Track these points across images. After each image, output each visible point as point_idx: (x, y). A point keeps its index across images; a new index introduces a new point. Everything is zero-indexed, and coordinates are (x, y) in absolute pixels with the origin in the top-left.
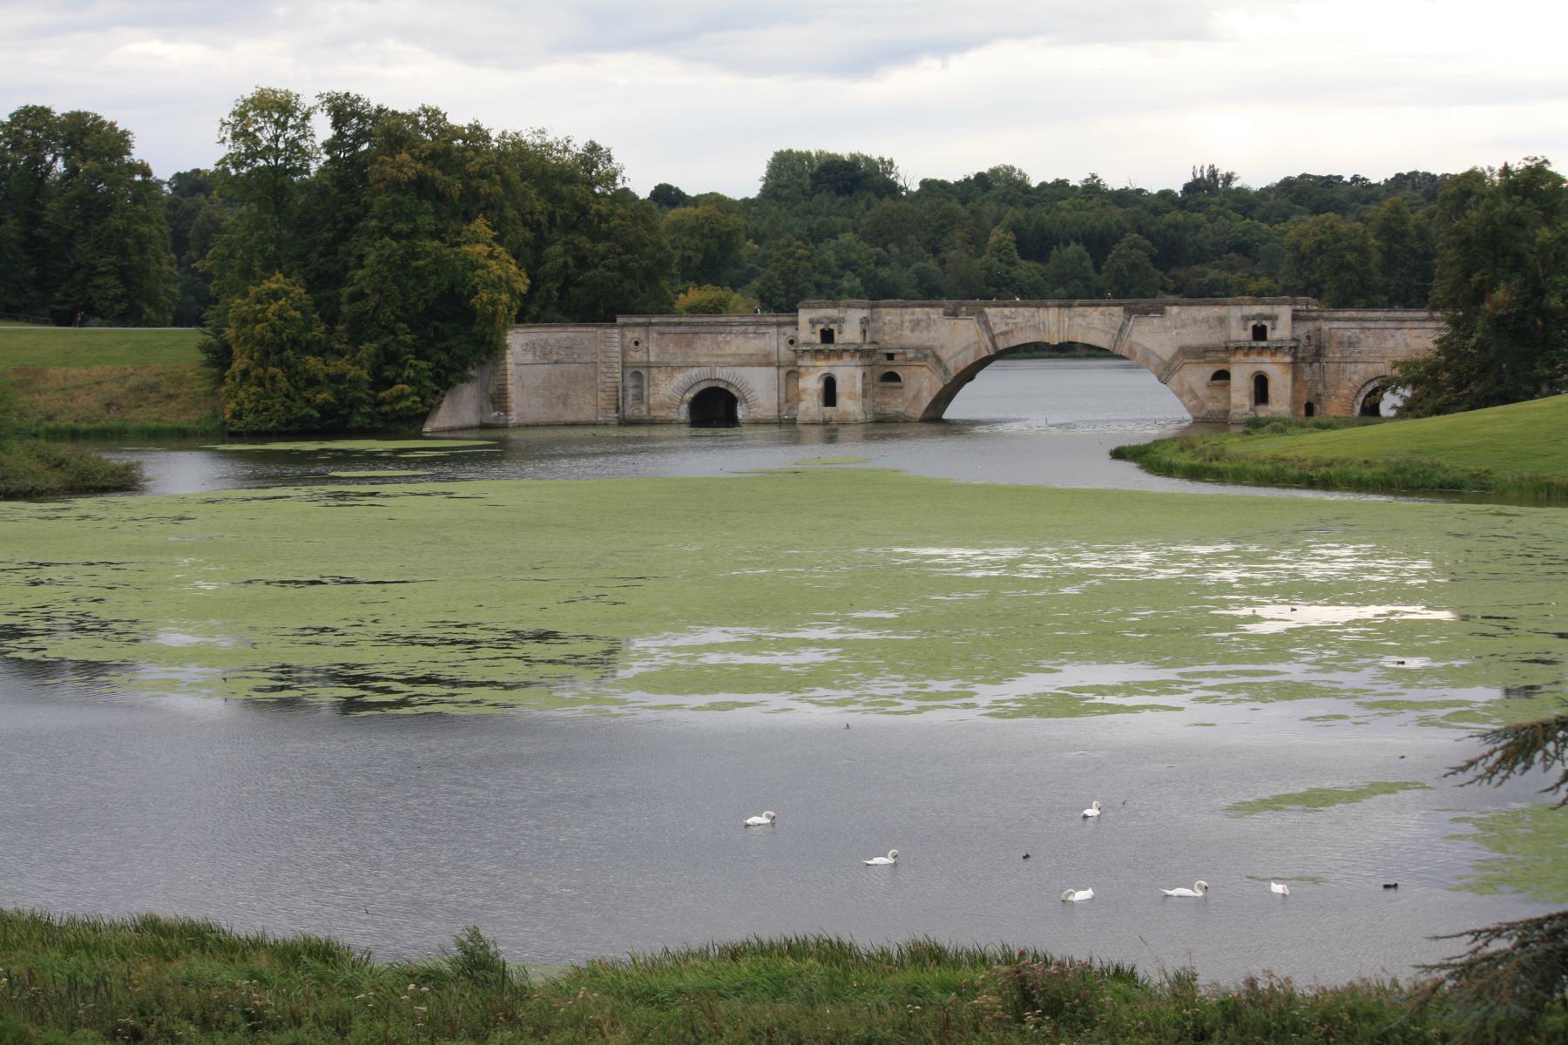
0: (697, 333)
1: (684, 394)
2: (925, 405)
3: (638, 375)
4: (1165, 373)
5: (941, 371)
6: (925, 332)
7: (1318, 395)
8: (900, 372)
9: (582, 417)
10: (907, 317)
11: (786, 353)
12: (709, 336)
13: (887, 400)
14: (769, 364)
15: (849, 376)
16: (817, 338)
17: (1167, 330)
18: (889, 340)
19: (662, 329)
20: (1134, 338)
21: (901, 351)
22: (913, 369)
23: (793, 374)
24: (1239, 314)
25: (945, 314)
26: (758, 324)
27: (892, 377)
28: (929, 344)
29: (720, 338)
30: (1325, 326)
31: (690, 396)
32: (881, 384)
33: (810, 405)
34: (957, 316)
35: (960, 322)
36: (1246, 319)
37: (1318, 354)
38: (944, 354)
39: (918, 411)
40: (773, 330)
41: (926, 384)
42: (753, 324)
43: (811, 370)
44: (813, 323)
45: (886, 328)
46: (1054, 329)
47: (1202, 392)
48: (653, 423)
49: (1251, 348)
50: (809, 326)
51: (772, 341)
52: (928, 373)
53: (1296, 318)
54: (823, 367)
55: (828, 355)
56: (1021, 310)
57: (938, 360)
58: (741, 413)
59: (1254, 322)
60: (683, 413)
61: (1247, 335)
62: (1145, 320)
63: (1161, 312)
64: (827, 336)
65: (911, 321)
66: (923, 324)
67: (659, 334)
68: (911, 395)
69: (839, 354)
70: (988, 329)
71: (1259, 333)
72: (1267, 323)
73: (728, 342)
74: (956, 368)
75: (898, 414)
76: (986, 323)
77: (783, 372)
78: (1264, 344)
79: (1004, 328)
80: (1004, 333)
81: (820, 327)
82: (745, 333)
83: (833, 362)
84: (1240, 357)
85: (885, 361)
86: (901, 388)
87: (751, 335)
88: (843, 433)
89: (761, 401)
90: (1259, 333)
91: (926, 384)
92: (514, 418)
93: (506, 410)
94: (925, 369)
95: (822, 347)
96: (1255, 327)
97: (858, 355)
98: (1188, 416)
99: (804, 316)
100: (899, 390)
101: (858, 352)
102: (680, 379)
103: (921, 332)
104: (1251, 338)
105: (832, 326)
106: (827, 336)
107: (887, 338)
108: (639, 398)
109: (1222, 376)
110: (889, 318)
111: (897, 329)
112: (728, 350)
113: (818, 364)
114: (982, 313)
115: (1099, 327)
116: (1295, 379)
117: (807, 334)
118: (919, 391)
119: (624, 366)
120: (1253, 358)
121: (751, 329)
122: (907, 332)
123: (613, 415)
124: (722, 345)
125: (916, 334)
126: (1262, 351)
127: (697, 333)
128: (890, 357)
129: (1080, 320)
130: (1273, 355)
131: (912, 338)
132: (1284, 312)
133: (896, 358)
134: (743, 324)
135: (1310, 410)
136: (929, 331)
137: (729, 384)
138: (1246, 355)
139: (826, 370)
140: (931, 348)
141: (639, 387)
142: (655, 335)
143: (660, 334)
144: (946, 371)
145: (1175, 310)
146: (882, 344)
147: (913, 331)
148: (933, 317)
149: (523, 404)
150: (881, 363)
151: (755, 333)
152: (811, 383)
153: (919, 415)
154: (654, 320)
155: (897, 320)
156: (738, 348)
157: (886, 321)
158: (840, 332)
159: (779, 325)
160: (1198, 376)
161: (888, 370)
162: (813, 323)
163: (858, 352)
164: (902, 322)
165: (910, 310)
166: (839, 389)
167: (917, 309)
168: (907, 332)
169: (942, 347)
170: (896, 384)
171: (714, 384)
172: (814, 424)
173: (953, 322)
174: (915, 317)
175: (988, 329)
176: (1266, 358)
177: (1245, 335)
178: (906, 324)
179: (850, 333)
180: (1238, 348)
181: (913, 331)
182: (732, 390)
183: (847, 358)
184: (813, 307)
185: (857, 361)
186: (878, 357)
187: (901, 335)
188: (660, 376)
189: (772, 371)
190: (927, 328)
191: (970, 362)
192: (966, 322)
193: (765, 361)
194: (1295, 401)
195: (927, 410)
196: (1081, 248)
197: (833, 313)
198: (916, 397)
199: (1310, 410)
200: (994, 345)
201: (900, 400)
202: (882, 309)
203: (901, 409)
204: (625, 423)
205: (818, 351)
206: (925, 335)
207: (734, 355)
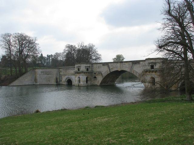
9: (52, 84)
16: (77, 70)
19: (63, 69)
20: (134, 69)
24: (148, 62)
27: (95, 77)
31: (66, 80)
38: (103, 73)
44: (77, 67)
46: (119, 67)
49: (150, 71)
54: (78, 75)
56: (114, 64)
57: (102, 74)
58: (73, 84)
59: (151, 64)
61: (149, 68)
64: (79, 69)
70: (109, 68)
71: (152, 67)
78: (153, 70)
79: (112, 68)
80: (112, 69)
81: (78, 68)
83: (80, 74)
84: (148, 73)
85: (94, 74)
88: (82, 88)
90: (152, 67)
91: (100, 79)
92: (38, 83)
99: (76, 66)
104: (150, 68)
106: (79, 69)
112: (71, 72)
115: (127, 67)
117: (76, 70)
120: (151, 73)
123: (56, 83)
126: (153, 71)
128: (95, 73)
129: (124, 65)
131: (98, 70)
134: (71, 68)
138: (149, 73)
139: (79, 76)
143: (63, 70)
147: (98, 68)
153: (99, 84)
161: (95, 76)
165: (98, 65)
168: (97, 69)
175: (109, 68)
176: (154, 74)
178: (97, 67)
180: (147, 71)
181: (98, 68)
188: (63, 77)
191: (106, 75)
195: (101, 83)
197: (79, 65)
200: (110, 71)
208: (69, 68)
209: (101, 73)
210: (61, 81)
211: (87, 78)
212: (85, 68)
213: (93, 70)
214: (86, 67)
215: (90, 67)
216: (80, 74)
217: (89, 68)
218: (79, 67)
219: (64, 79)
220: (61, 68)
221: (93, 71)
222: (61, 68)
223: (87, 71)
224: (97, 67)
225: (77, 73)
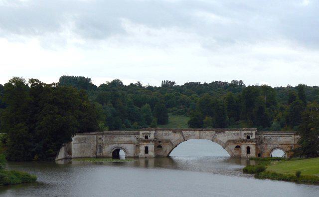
3: (100, 146)
4: (225, 146)
7: (262, 152)
11: (136, 141)
14: (131, 144)
15: (151, 147)
17: (225, 136)
18: (160, 138)
23: (138, 146)
27: (160, 146)
30: (263, 136)
33: (142, 153)
36: (245, 134)
37: (261, 142)
38: (172, 141)
39: (166, 155)
40: (133, 135)
44: (143, 134)
47: (233, 151)
48: (103, 157)
51: (133, 138)
53: (256, 134)
54: (145, 144)
55: (147, 142)
60: (111, 155)
61: (245, 138)
62: (220, 134)
63: (224, 132)
64: (146, 137)
69: (149, 141)
70: (183, 136)
72: (250, 135)
75: (162, 156)
76: (182, 134)
77: (135, 145)
79: (186, 135)
81: (145, 135)
83: (148, 143)
84: (244, 143)
92: (73, 156)
93: (71, 155)
95: (146, 140)
96: (247, 136)
98: (229, 156)
99: (141, 132)
101: (154, 141)
102: (111, 146)
106: (146, 137)
108: (101, 151)
109: (238, 147)
112: (123, 140)
114: (181, 132)
116: (256, 148)
117: (141, 136)
119: (97, 144)
120: (247, 143)
128: (160, 142)
130: (252, 142)
132: (254, 133)
135: (259, 155)
141: (101, 149)
145: (227, 131)
149: (75, 153)
152: (142, 148)
159: (134, 134)
160: (233, 147)
163: (154, 141)
166: (149, 150)
172: (143, 158)
175: (183, 136)
177: (245, 138)
179: (152, 137)
183: (151, 143)
185: (153, 143)
188: (106, 146)
189: (133, 145)
190: (168, 135)
193: (130, 143)
194: (256, 153)
196: (149, 105)
199: (259, 155)
204: (97, 157)
205: (144, 141)
218: (148, 134)
219: (108, 150)
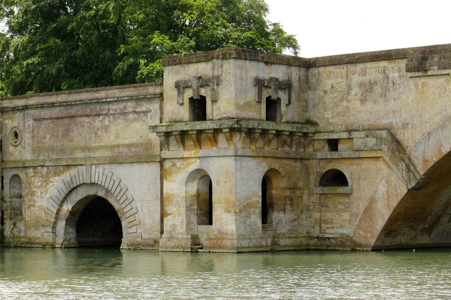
0: (73, 117)
1: (61, 205)
2: (380, 223)
5: (403, 165)
6: (381, 100)
8: (346, 169)
10: (356, 79)
12: (86, 119)
13: (329, 216)
16: (185, 112)
21: (345, 135)
22: (365, 164)
25: (408, 70)
26: (138, 99)
28: (385, 122)
29: (97, 122)
31: (68, 207)
32: (319, 190)
34: (426, 71)
35: (431, 82)
41: (382, 188)
42: (131, 98)
43: (179, 163)
44: (180, 87)
45: (328, 99)
50: (175, 92)
52: (385, 171)
65: (361, 85)
66: (378, 89)
67: (35, 120)
68: (360, 206)
73: (106, 129)
74: (426, 161)
81: (189, 94)
82: (124, 113)
85: (325, 153)
86: (348, 195)
87: (131, 116)
89: (140, 216)
94: (380, 164)
97: (238, 138)
100: (345, 200)
103: (375, 102)
105: (203, 92)
107: (328, 115)
110: (330, 82)
111: (342, 100)
112: (109, 139)
113: (186, 154)
118: (372, 200)
121: (130, 106)
122: (355, 104)
124: (99, 133)
125: (369, 105)
127: (73, 117)
128: (333, 144)
133: (340, 146)
134: (118, 100)
136: (386, 100)
137: (107, 191)
139: (195, 165)
140: (389, 130)
142: (31, 122)
143: (37, 120)
144: (410, 167)
146: (322, 125)
147: (363, 101)
148: (391, 75)
150: (319, 155)
151: (134, 112)
153: (372, 242)
154: (32, 101)
155: (342, 85)
156: (117, 137)
157: (328, 88)
158: (214, 101)
162: (180, 87)
164: (349, 88)
167: (369, 65)
168: (355, 104)
169: (405, 126)
170: (341, 190)
171: (92, 192)
173: (420, 81)
174: (366, 79)
178: (356, 90)
181: (363, 101)
182: (111, 201)
184: (180, 63)
186: (317, 145)
187: (348, 108)
192: (442, 80)
198: (369, 211)
201: (346, 216)
202: (322, 69)
203: (347, 231)
206: (380, 107)
207: (112, 147)
208: (99, 102)
209: (392, 135)
210: (18, 213)
211: (266, 183)
212: (252, 94)
213: (313, 115)
214: (259, 83)
215: (286, 86)
216: (214, 141)
217: (283, 96)
218: (203, 82)
220: (15, 109)
221: (309, 122)
222: (15, 109)
223: (267, 119)
224: (356, 90)
225: (183, 134)
